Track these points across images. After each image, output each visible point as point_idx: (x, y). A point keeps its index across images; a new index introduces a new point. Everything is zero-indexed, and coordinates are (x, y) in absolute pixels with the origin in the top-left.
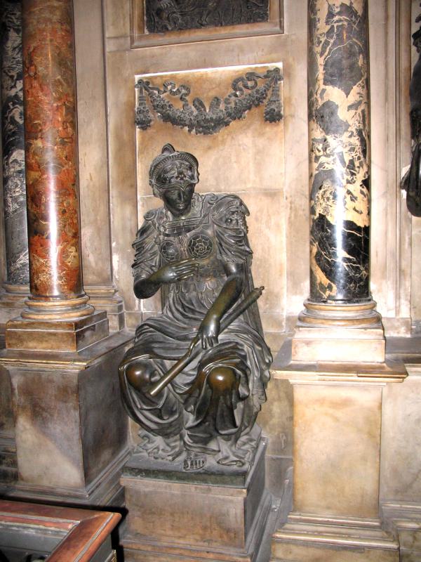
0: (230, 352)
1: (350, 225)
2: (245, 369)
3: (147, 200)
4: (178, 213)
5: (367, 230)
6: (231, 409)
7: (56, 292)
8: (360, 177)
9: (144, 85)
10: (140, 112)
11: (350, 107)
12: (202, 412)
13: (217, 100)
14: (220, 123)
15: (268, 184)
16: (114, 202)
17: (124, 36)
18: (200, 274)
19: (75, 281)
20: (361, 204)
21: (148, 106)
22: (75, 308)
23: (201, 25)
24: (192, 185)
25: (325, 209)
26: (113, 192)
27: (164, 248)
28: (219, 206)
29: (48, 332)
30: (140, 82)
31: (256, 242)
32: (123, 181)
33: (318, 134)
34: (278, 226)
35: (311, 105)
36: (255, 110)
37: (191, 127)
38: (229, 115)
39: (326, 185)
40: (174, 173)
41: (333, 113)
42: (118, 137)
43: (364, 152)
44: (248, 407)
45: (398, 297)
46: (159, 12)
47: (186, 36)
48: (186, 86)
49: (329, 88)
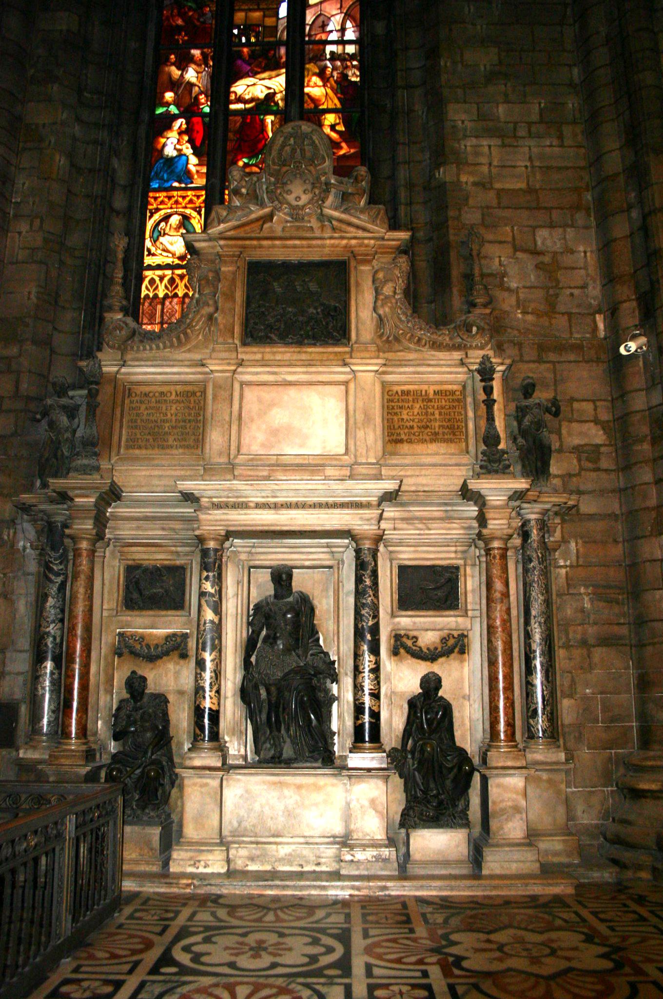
0: (157, 762)
1: (210, 709)
2: (162, 768)
3: (119, 691)
4: (136, 701)
5: (218, 712)
6: (157, 790)
7: (73, 736)
8: (215, 689)
9: (121, 635)
10: (119, 648)
12: (142, 793)
13: (157, 646)
14: (158, 657)
15: (179, 688)
16: (102, 692)
17: (113, 609)
18: (145, 731)
19: (83, 731)
20: (215, 701)
21: (123, 646)
22: (84, 744)
23: (151, 609)
24: (144, 690)
26: (102, 688)
27: (129, 717)
28: (155, 699)
29: (71, 754)
30: (119, 633)
31: (173, 717)
32: (107, 682)
33: (199, 671)
34: (184, 709)
35: (197, 658)
36: (176, 652)
37: (144, 658)
39: (201, 692)
40: (137, 684)
42: (106, 659)
43: (217, 679)
44: (164, 792)
45: (239, 744)
46: (131, 600)
47: (144, 613)
48: (142, 637)
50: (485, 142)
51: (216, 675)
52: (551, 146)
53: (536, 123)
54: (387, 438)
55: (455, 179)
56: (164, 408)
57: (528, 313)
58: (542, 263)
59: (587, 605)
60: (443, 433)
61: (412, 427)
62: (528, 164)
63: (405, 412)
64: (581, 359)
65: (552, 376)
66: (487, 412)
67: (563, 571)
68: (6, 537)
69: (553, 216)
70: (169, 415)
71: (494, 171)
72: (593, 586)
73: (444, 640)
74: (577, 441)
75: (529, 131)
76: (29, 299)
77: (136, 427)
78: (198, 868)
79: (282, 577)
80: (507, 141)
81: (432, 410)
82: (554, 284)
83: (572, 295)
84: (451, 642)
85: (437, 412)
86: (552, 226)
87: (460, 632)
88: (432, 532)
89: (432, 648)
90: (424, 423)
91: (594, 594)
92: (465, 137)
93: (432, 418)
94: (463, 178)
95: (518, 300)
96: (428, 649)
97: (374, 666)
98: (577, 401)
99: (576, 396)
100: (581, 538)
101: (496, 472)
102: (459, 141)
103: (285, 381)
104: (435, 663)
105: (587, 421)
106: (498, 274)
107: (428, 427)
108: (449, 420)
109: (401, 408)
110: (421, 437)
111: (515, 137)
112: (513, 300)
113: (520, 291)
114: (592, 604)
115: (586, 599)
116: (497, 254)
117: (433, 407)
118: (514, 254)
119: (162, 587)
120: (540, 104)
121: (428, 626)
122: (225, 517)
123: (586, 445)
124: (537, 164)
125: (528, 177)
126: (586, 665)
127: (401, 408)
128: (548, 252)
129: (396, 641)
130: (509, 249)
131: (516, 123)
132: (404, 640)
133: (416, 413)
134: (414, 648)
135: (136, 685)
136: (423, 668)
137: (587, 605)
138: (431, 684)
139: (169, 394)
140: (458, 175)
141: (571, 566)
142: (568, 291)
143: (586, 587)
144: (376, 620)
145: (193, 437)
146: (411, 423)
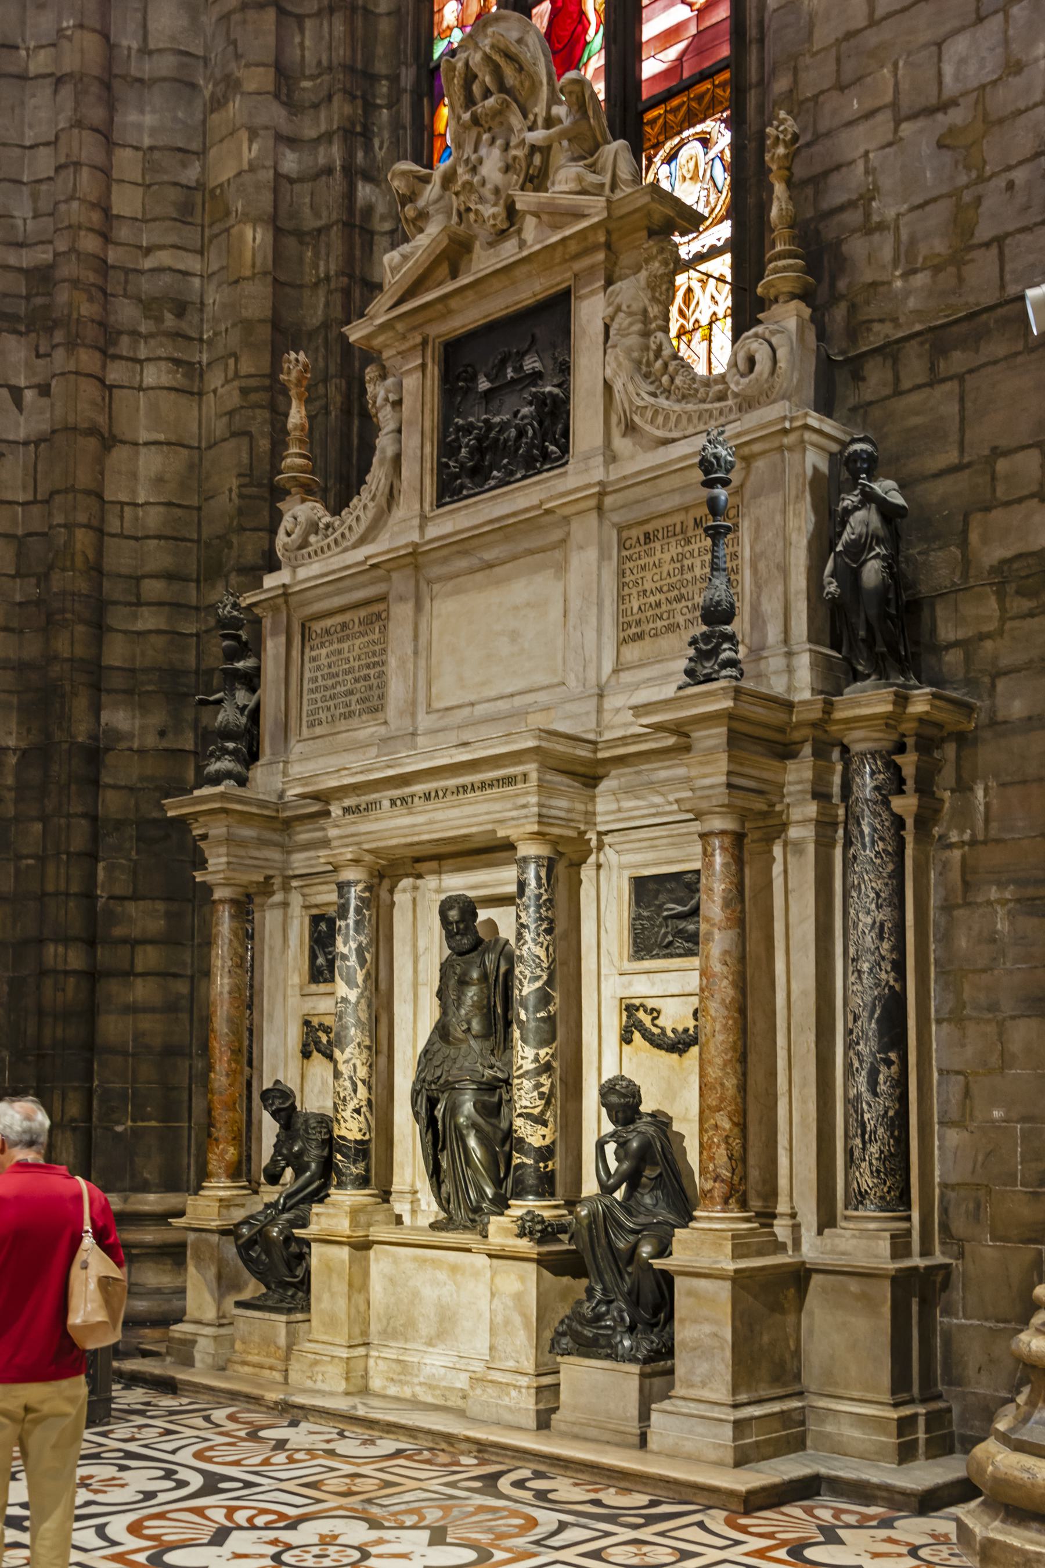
54: (621, 635)
57: (914, 271)
59: (1002, 925)
61: (658, 605)
63: (648, 575)
64: (1020, 347)
65: (956, 408)
67: (957, 853)
72: (1017, 882)
74: (998, 553)
82: (974, 174)
83: (1011, 186)
89: (680, 1029)
90: (676, 592)
91: (1018, 901)
96: (674, 1031)
98: (1007, 453)
99: (1004, 443)
100: (996, 776)
105: (1020, 500)
107: (682, 596)
109: (643, 568)
110: (671, 621)
114: (1011, 924)
115: (1001, 912)
118: (896, 131)
123: (1020, 556)
126: (994, 1060)
127: (643, 568)
133: (665, 575)
137: (1002, 925)
141: (973, 843)
142: (1001, 182)
143: (1001, 885)
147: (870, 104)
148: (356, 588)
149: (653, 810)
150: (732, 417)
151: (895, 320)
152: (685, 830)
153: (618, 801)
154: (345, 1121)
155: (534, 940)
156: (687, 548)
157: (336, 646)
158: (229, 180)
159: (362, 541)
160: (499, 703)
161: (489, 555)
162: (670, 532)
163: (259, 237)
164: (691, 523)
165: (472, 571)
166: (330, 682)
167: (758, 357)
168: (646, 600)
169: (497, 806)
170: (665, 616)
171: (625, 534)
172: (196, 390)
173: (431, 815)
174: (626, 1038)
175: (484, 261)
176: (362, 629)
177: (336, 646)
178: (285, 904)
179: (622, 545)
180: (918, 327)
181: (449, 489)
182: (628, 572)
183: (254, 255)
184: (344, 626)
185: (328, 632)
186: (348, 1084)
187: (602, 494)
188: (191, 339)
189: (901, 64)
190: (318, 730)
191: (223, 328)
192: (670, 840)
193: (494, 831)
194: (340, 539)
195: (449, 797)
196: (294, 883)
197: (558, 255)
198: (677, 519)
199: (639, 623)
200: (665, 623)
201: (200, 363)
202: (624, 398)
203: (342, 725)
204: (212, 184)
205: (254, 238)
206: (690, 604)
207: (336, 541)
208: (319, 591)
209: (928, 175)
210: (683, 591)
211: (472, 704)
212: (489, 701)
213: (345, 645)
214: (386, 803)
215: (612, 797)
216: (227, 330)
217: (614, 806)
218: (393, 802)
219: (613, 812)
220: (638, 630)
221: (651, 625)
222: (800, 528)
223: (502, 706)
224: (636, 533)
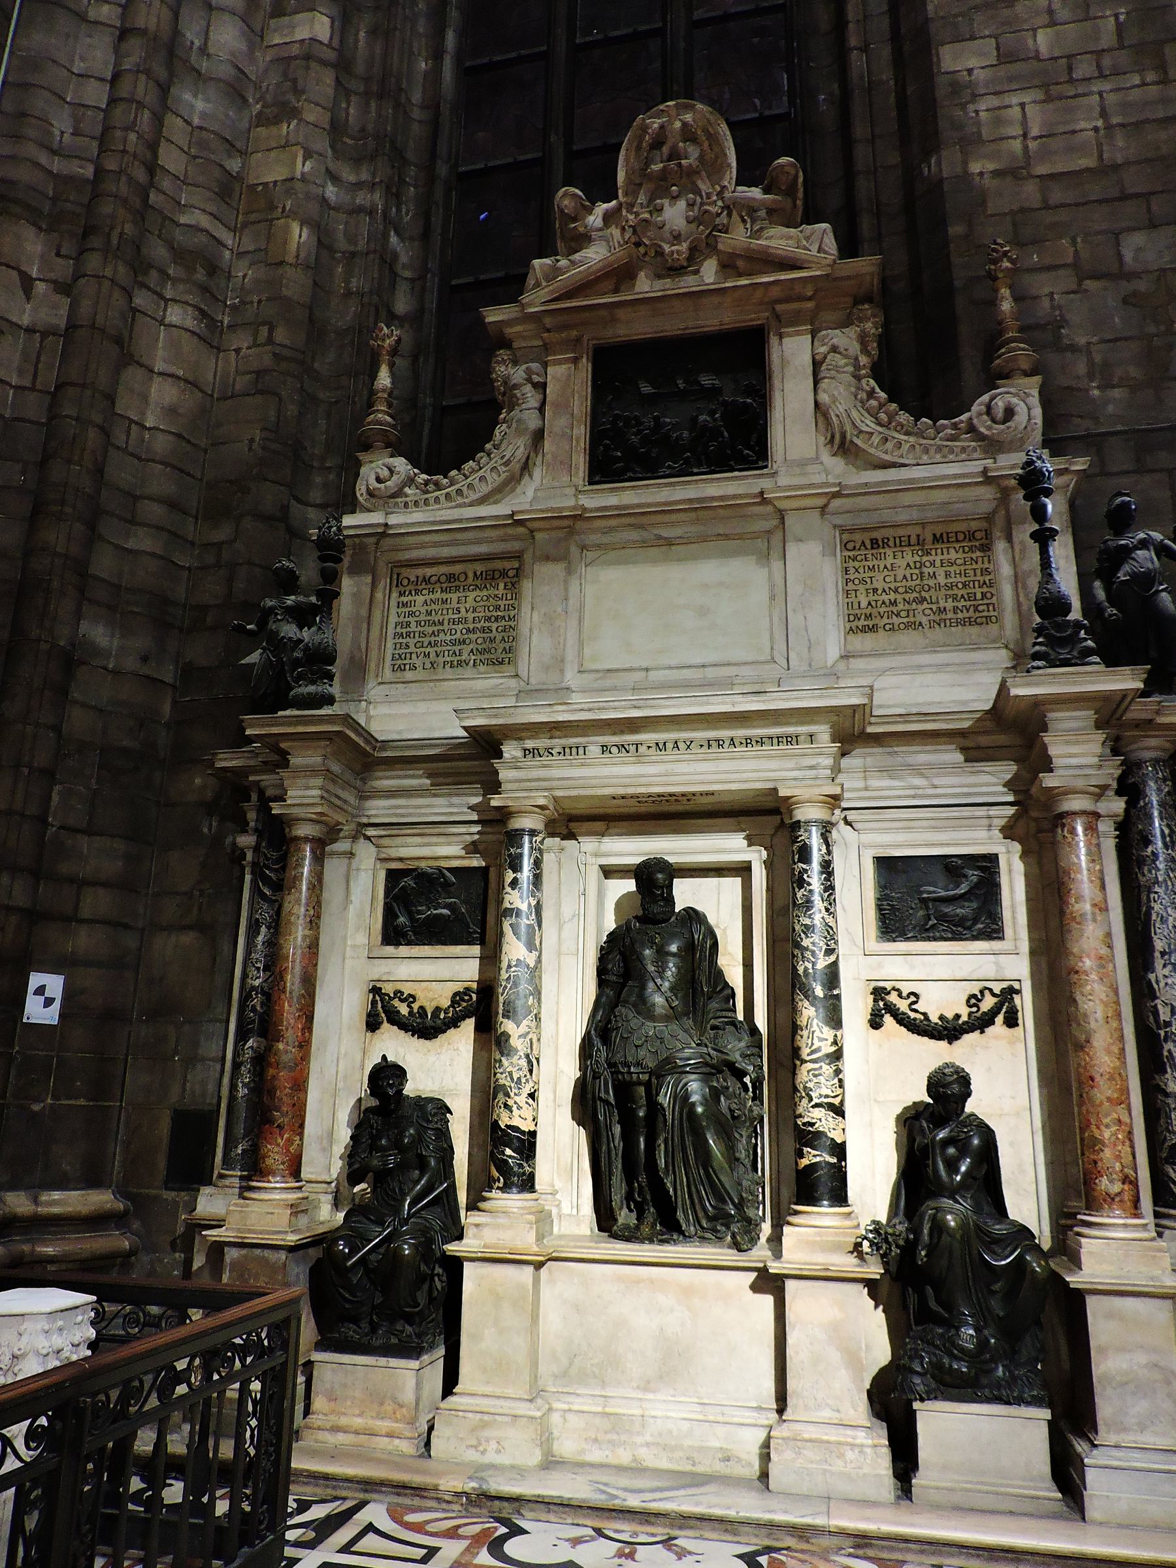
5: (533, 1134)
11: (520, 1037)
13: (438, 1009)
20: (527, 1113)
25: (498, 1116)
38: (444, 1024)
41: (507, 1040)
49: (505, 1021)
50: (1015, 100)
51: (530, 1062)
52: (1144, 84)
53: (1110, 50)
54: (848, 626)
55: (959, 170)
56: (455, 600)
57: (1113, 387)
58: (1135, 294)
60: (955, 610)
61: (894, 603)
62: (1100, 123)
66: (1041, 554)
68: (206, 830)
69: (1154, 208)
70: (463, 610)
71: (1032, 145)
73: (973, 1000)
75: (1099, 67)
76: (250, 449)
77: (408, 635)
78: (483, 1453)
79: (653, 879)
80: (1055, 90)
81: (931, 570)
82: (1162, 328)
84: (988, 1003)
85: (941, 573)
86: (1153, 225)
87: (1005, 985)
88: (939, 791)
90: (915, 595)
92: (975, 97)
93: (932, 582)
94: (975, 167)
95: (1091, 363)
96: (941, 1018)
97: (834, 1048)
101: (1066, 663)
102: (963, 106)
103: (659, 537)
104: (957, 1043)
106: (1048, 324)
108: (965, 585)
110: (912, 620)
111: (1071, 81)
112: (1081, 368)
113: (1093, 348)
116: (1046, 290)
117: (933, 564)
118: (1080, 285)
119: (446, 906)
120: (1116, 16)
121: (942, 974)
122: (542, 773)
124: (1115, 120)
125: (1099, 145)
128: (1148, 272)
129: (875, 1001)
130: (1066, 279)
131: (1069, 57)
132: (893, 998)
133: (900, 578)
134: (913, 1015)
135: (387, 1077)
136: (935, 1054)
138: (949, 1089)
139: (462, 578)
140: (965, 163)
144: (832, 958)
145: (502, 645)
146: (892, 596)
147: (1048, 261)
148: (479, 542)
149: (911, 792)
150: (975, 456)
151: (1096, 420)
152: (945, 815)
153: (865, 779)
154: (519, 1108)
155: (827, 910)
156: (925, 558)
157: (438, 595)
158: (275, 182)
159: (482, 501)
160: (685, 671)
161: (665, 533)
162: (903, 543)
163: (304, 235)
164: (929, 538)
165: (644, 544)
166: (429, 630)
167: (1017, 409)
168: (876, 597)
169: (773, 764)
170: (903, 614)
171: (846, 537)
172: (215, 344)
173: (669, 767)
174: (875, 1023)
175: (645, 285)
176: (478, 582)
177: (438, 595)
178: (351, 855)
179: (845, 546)
180: (1119, 428)
181: (603, 470)
182: (852, 571)
183: (298, 247)
184: (451, 577)
185: (427, 580)
186: (523, 1063)
187: (836, 495)
188: (218, 300)
189: (1079, 240)
190: (409, 675)
191: (256, 299)
192: (932, 823)
193: (775, 790)
194: (453, 494)
195: (695, 748)
196: (371, 832)
197: (759, 293)
198: (914, 531)
199: (869, 617)
200: (905, 620)
201: (222, 322)
202: (846, 420)
203: (449, 673)
204: (252, 181)
205: (298, 235)
206: (934, 607)
207: (448, 496)
208: (427, 538)
209: (1117, 320)
210: (923, 594)
211: (647, 670)
212: (670, 668)
213: (454, 596)
214: (594, 750)
215: (862, 775)
216: (259, 302)
217: (861, 784)
218: (605, 748)
219: (859, 790)
220: (870, 623)
221: (885, 620)
222: (1067, 557)
223: (687, 674)
224: (866, 537)
